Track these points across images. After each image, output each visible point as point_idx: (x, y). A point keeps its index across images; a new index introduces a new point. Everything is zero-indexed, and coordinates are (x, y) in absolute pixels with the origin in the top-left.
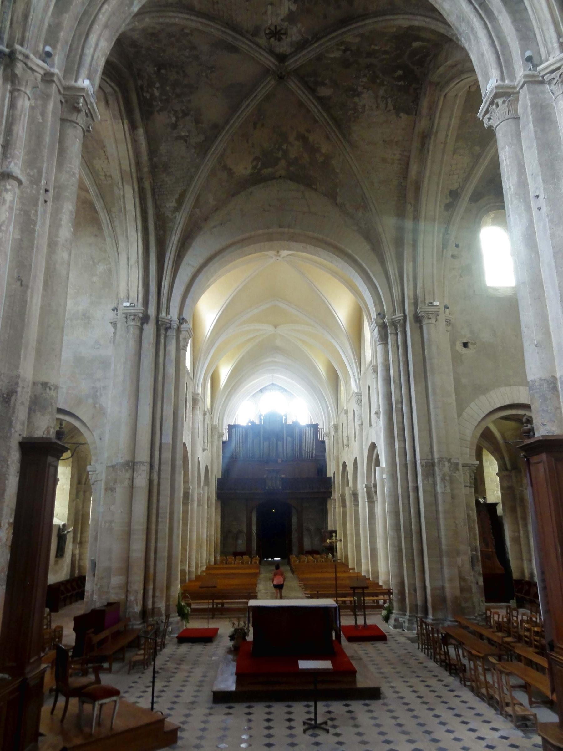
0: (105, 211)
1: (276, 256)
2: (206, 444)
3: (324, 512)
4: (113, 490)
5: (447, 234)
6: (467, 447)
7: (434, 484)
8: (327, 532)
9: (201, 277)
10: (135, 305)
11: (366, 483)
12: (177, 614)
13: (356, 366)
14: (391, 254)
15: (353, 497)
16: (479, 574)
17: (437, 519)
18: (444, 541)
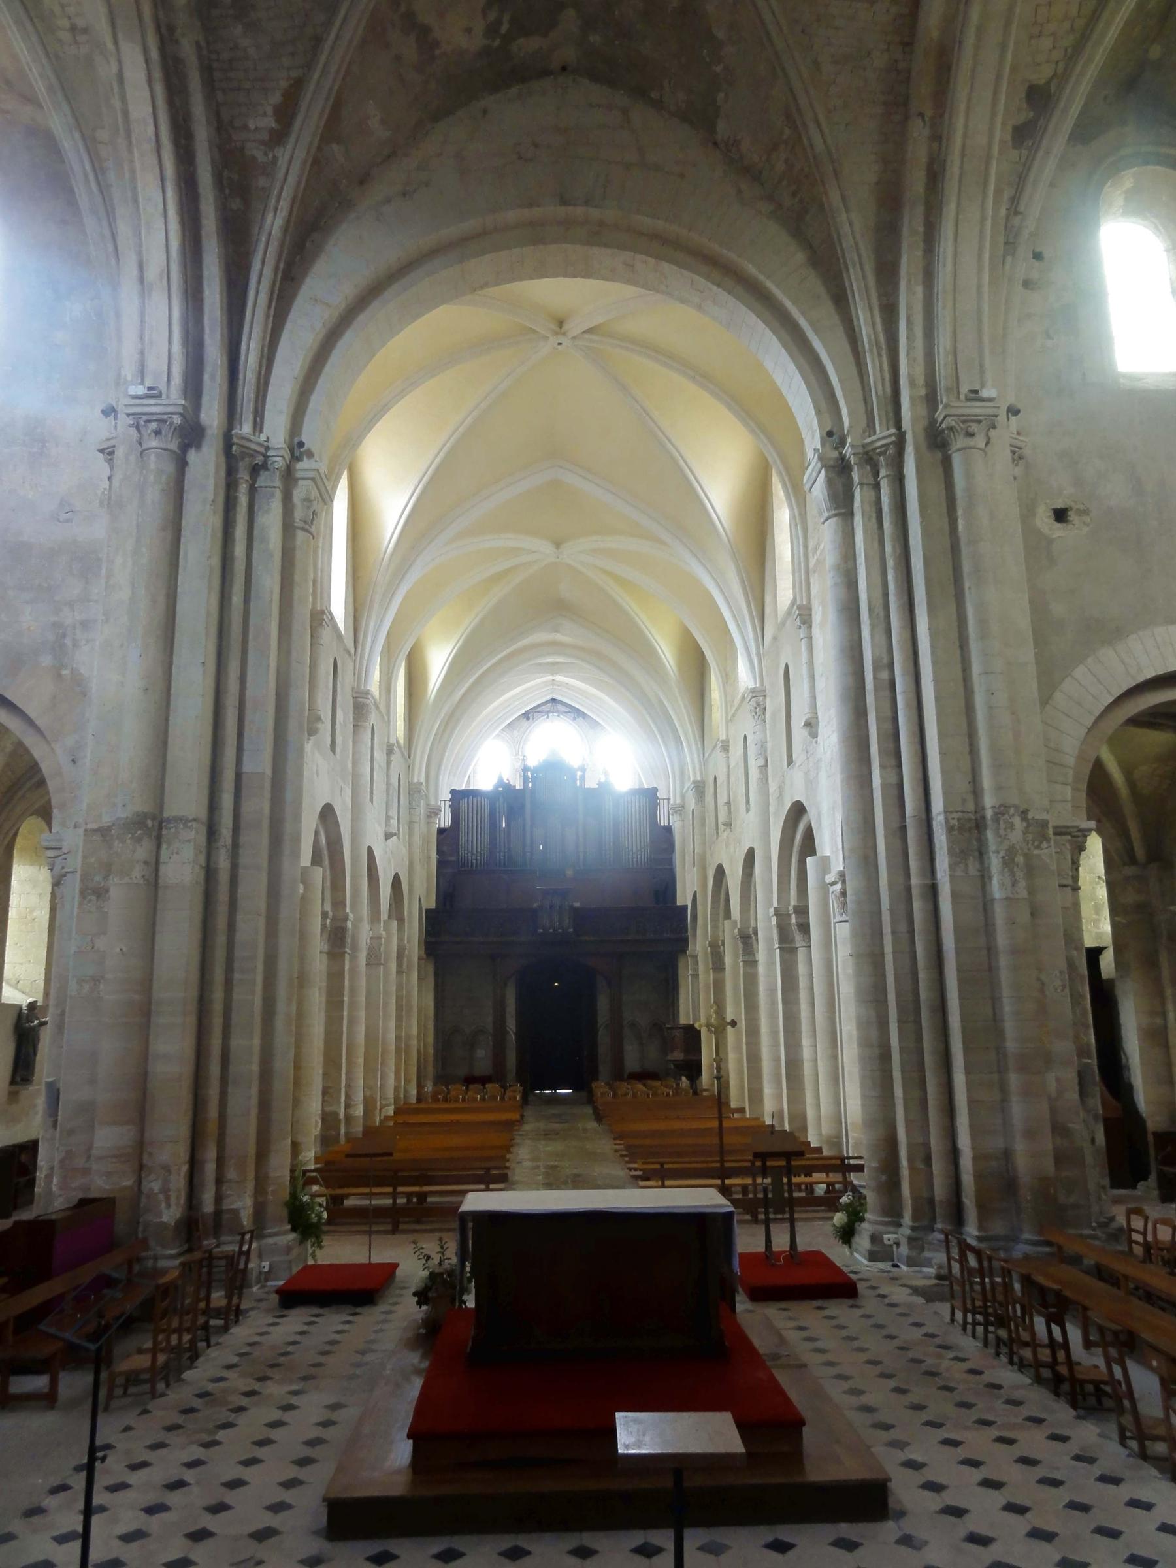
0: (77, 135)
1: (556, 333)
2: (394, 822)
3: (669, 988)
4: (100, 893)
5: (1017, 213)
6: (1065, 784)
7: (984, 877)
9: (349, 340)
10: (161, 392)
11: (775, 904)
12: (289, 1227)
13: (753, 624)
14: (862, 269)
15: (741, 946)
16: (1096, 1117)
17: (992, 968)
18: (1009, 1026)
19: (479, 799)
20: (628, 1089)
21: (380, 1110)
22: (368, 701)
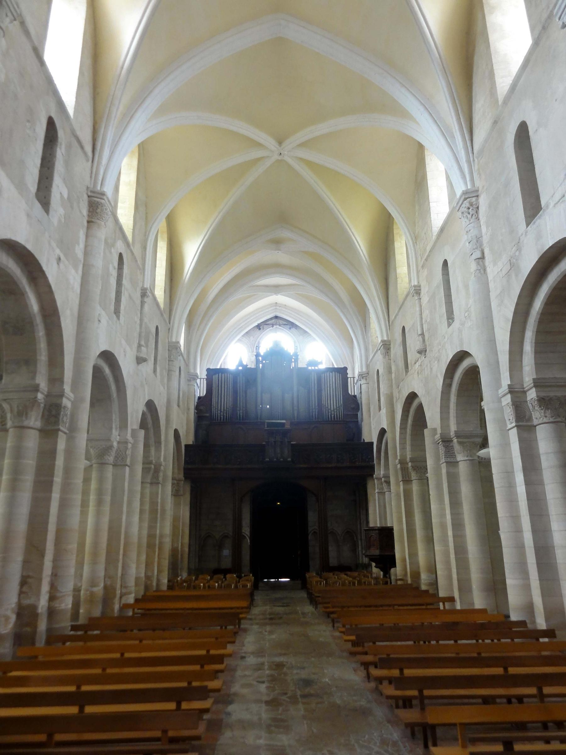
8: (373, 529)
15: (442, 449)
19: (226, 375)
20: (335, 578)
21: (121, 598)
22: (103, 201)
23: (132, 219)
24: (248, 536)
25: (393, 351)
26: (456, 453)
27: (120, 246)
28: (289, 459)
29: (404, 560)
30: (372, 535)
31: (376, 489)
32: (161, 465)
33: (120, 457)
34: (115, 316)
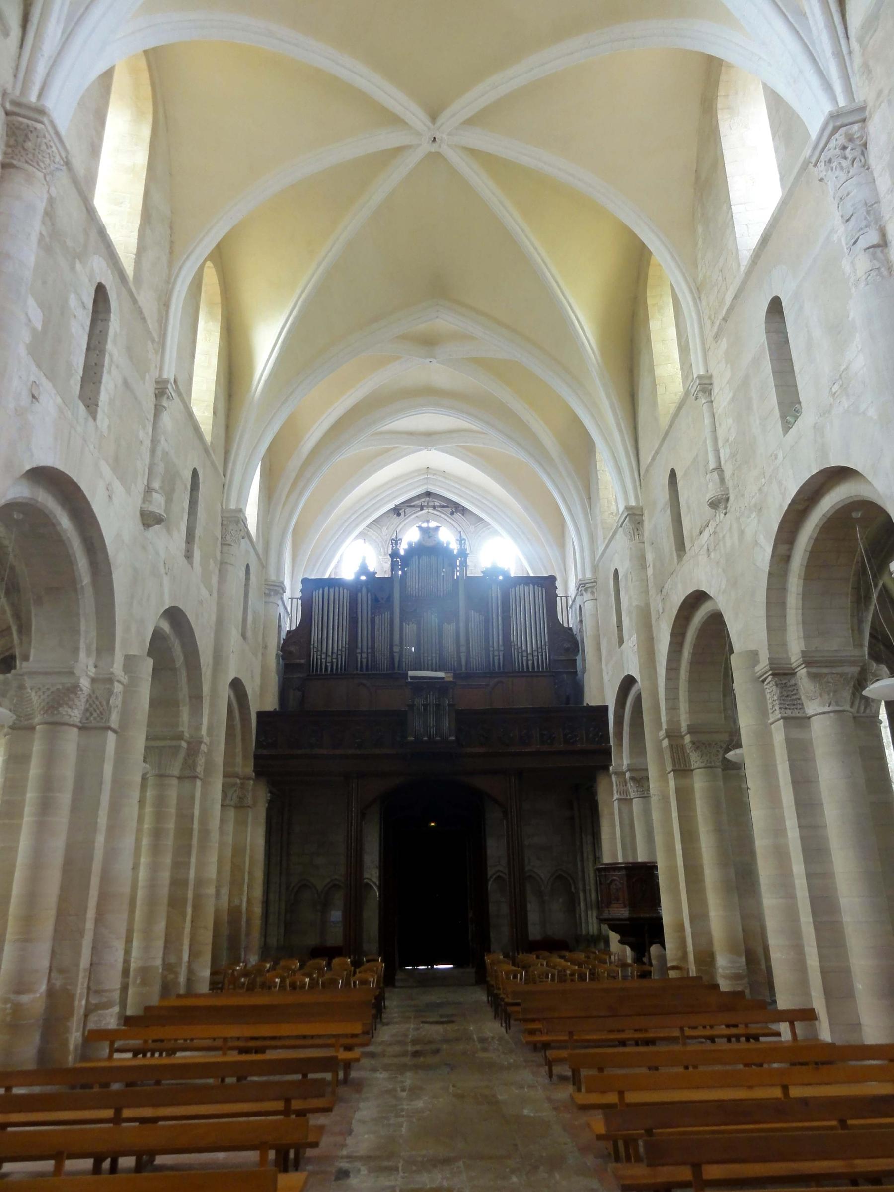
15: (771, 691)
20: (542, 965)
21: (86, 1016)
23: (135, 234)
24: (375, 884)
25: (647, 526)
26: (803, 697)
27: (103, 273)
28: (453, 738)
29: (681, 928)
30: (613, 880)
31: (615, 792)
32: (201, 742)
33: (95, 711)
34: (82, 408)
